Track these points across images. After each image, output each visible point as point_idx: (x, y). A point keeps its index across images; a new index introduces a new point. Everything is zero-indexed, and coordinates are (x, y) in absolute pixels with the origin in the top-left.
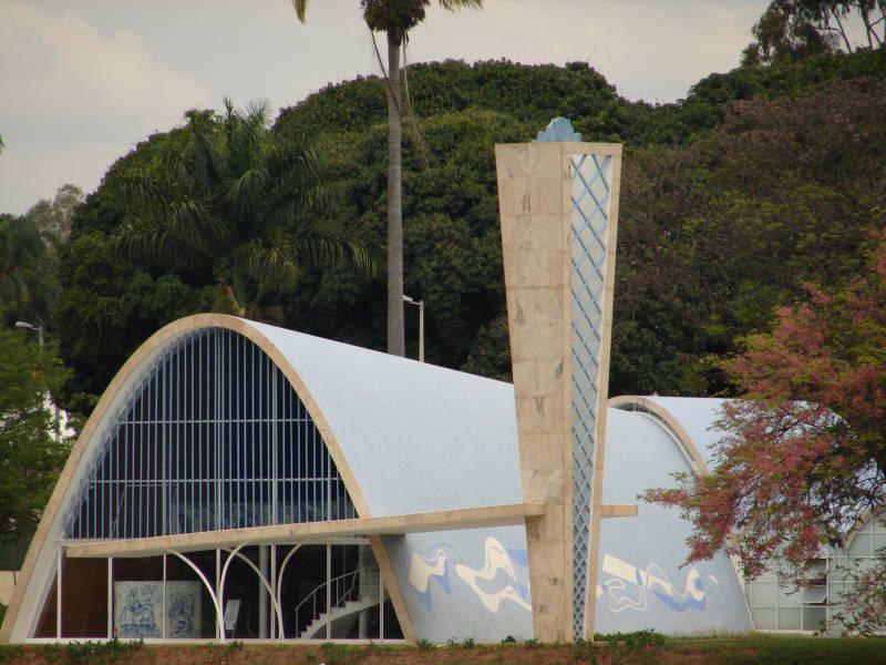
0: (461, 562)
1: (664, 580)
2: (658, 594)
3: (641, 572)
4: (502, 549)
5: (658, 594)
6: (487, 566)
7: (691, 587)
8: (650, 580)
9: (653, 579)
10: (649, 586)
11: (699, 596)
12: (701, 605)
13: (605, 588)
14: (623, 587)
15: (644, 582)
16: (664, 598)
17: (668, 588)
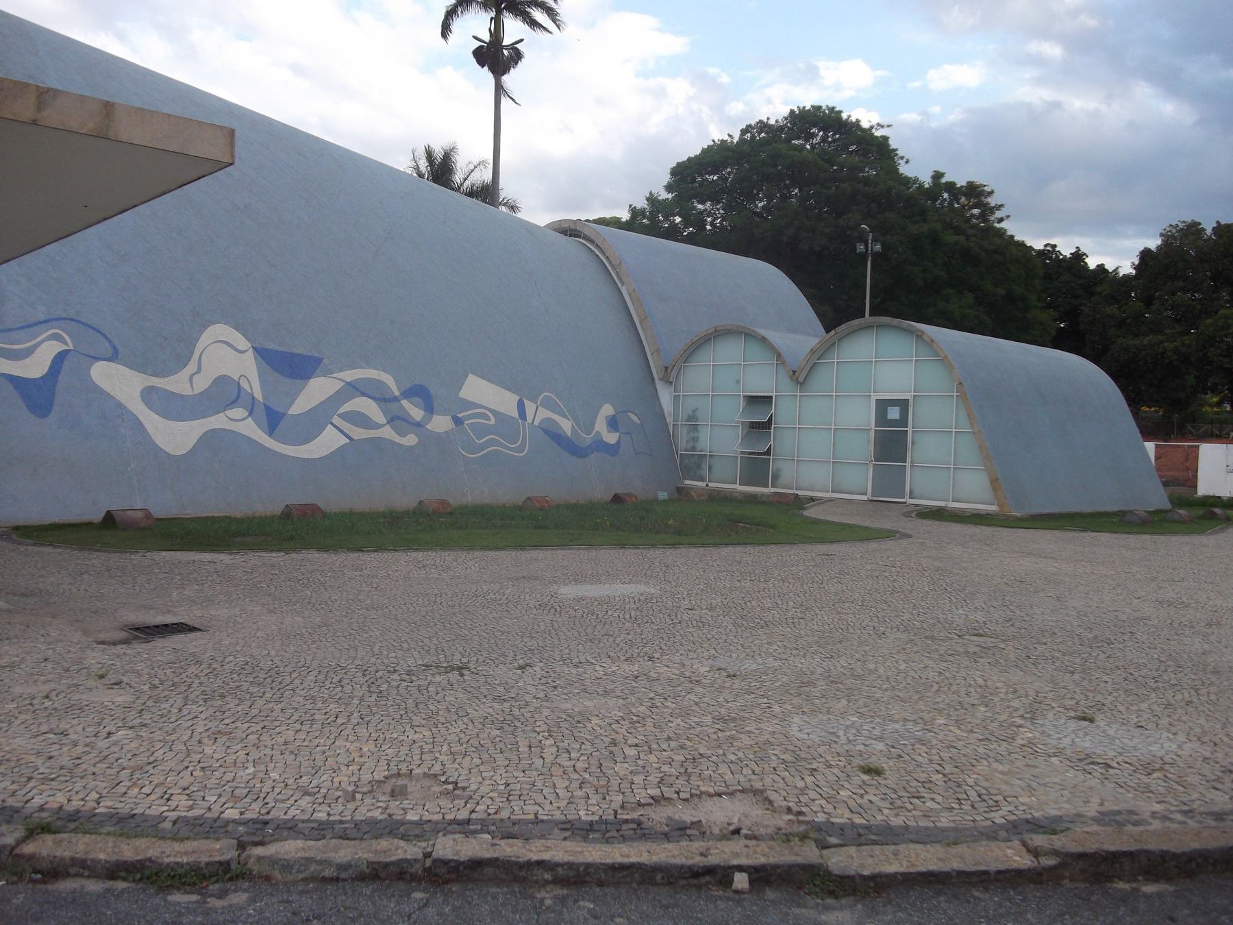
0: (114, 357)
1: (564, 416)
2: (546, 431)
3: (527, 403)
4: (242, 343)
5: (546, 431)
6: (192, 367)
7: (601, 426)
8: (537, 414)
9: (544, 413)
10: (536, 423)
11: (611, 438)
12: (613, 450)
13: (458, 421)
14: (493, 421)
15: (529, 418)
16: (556, 436)
17: (566, 426)
